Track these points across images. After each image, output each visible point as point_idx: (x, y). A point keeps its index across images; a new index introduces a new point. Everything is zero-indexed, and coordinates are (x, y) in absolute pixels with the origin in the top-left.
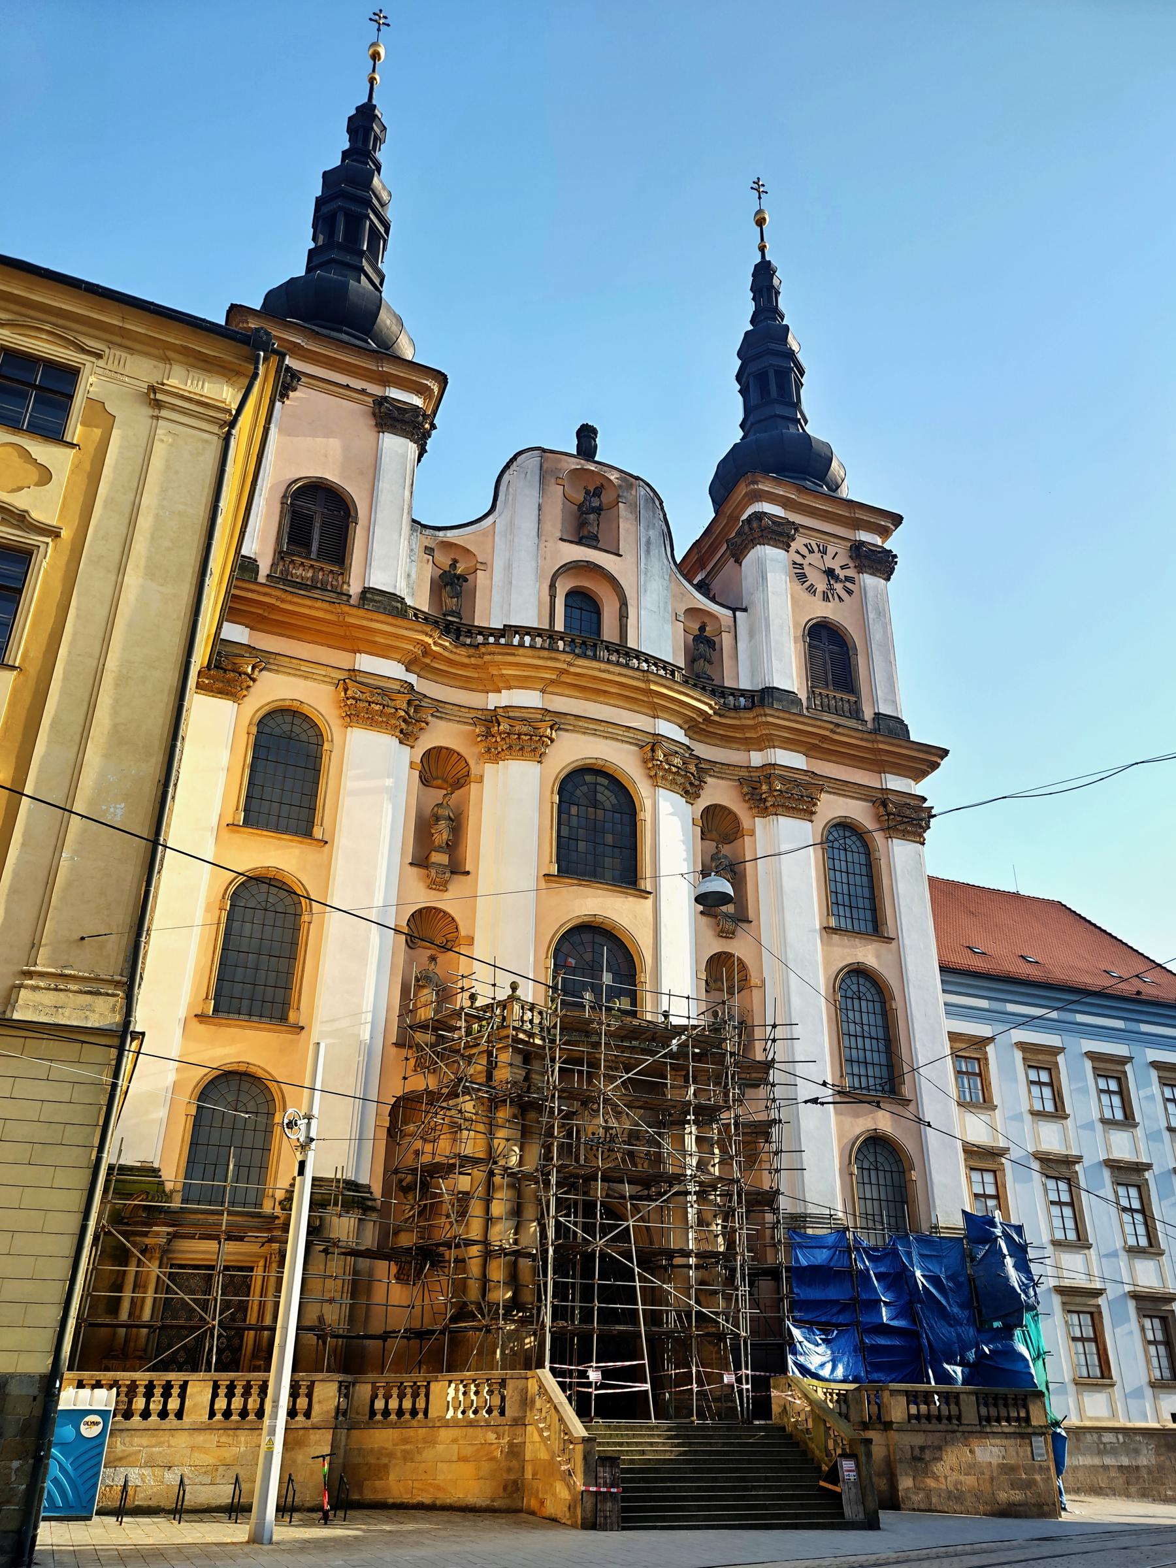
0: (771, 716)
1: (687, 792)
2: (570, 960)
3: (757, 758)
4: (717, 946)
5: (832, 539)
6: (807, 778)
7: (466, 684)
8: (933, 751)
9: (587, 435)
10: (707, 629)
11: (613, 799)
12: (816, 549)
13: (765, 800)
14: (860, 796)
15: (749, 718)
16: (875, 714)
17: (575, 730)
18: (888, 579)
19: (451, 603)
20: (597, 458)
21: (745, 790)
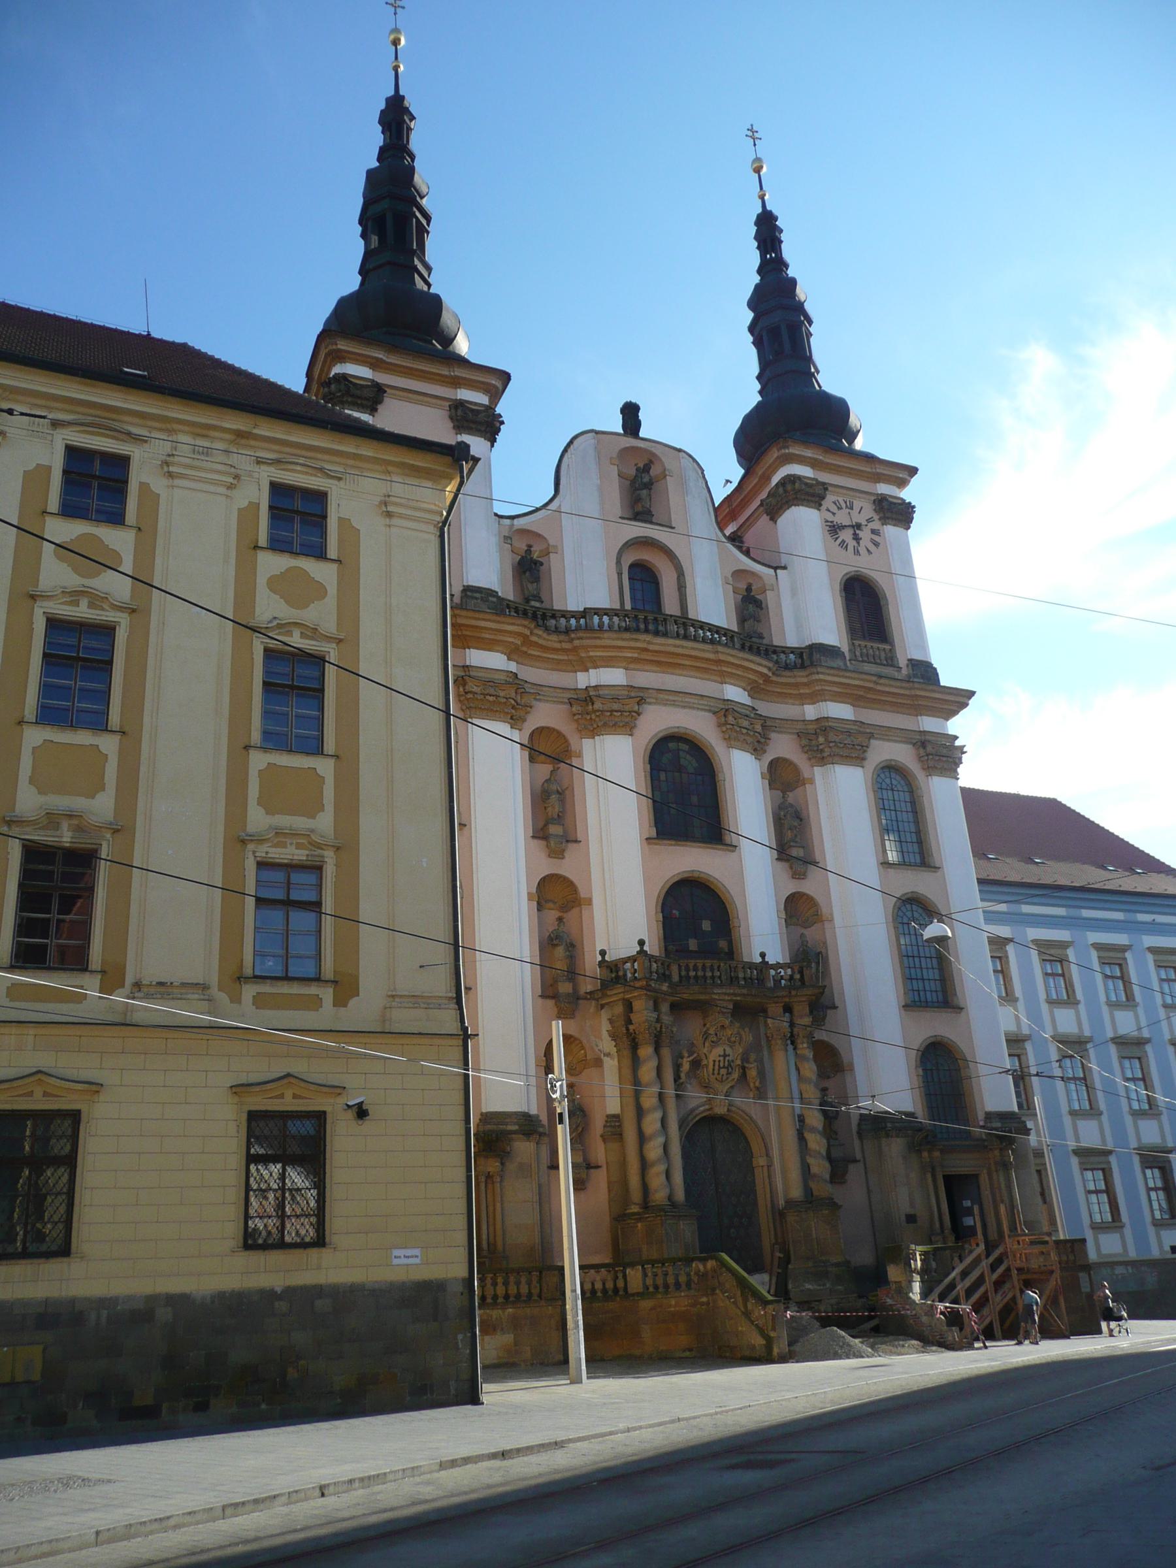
0: (822, 673)
1: (755, 750)
2: (674, 912)
3: (811, 712)
4: (791, 887)
5: (858, 494)
6: (856, 727)
7: (558, 666)
8: (963, 693)
9: (630, 412)
10: (753, 588)
11: (695, 765)
12: (844, 506)
13: (822, 751)
14: (900, 739)
15: (803, 677)
16: (909, 660)
17: (658, 702)
18: (908, 528)
19: (532, 587)
20: (641, 434)
21: (804, 742)
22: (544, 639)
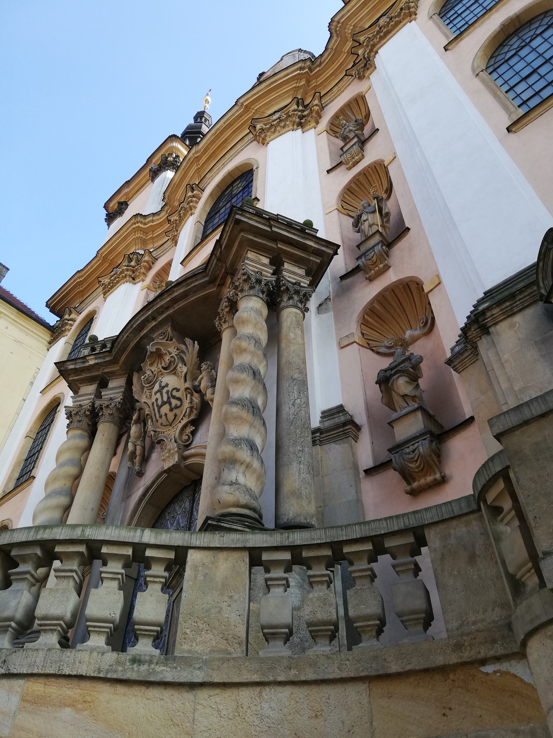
22: (158, 220)
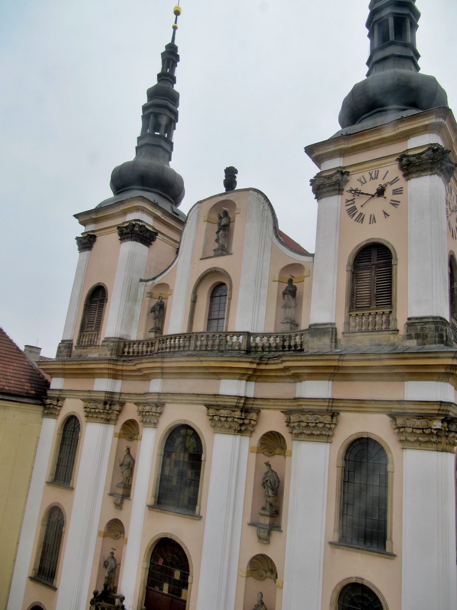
17: (174, 402)
